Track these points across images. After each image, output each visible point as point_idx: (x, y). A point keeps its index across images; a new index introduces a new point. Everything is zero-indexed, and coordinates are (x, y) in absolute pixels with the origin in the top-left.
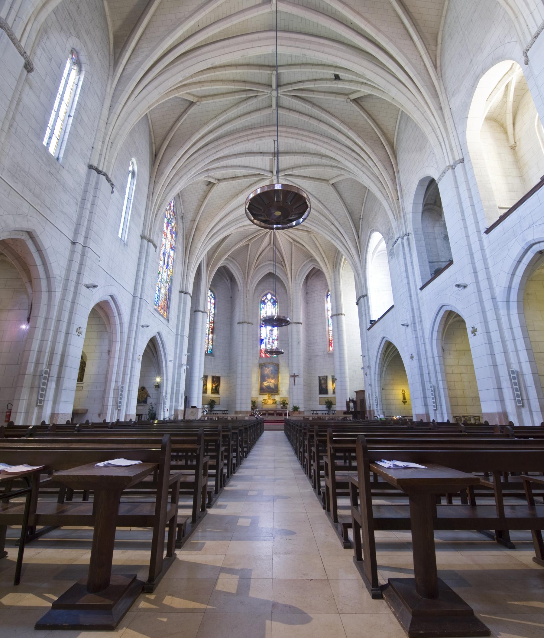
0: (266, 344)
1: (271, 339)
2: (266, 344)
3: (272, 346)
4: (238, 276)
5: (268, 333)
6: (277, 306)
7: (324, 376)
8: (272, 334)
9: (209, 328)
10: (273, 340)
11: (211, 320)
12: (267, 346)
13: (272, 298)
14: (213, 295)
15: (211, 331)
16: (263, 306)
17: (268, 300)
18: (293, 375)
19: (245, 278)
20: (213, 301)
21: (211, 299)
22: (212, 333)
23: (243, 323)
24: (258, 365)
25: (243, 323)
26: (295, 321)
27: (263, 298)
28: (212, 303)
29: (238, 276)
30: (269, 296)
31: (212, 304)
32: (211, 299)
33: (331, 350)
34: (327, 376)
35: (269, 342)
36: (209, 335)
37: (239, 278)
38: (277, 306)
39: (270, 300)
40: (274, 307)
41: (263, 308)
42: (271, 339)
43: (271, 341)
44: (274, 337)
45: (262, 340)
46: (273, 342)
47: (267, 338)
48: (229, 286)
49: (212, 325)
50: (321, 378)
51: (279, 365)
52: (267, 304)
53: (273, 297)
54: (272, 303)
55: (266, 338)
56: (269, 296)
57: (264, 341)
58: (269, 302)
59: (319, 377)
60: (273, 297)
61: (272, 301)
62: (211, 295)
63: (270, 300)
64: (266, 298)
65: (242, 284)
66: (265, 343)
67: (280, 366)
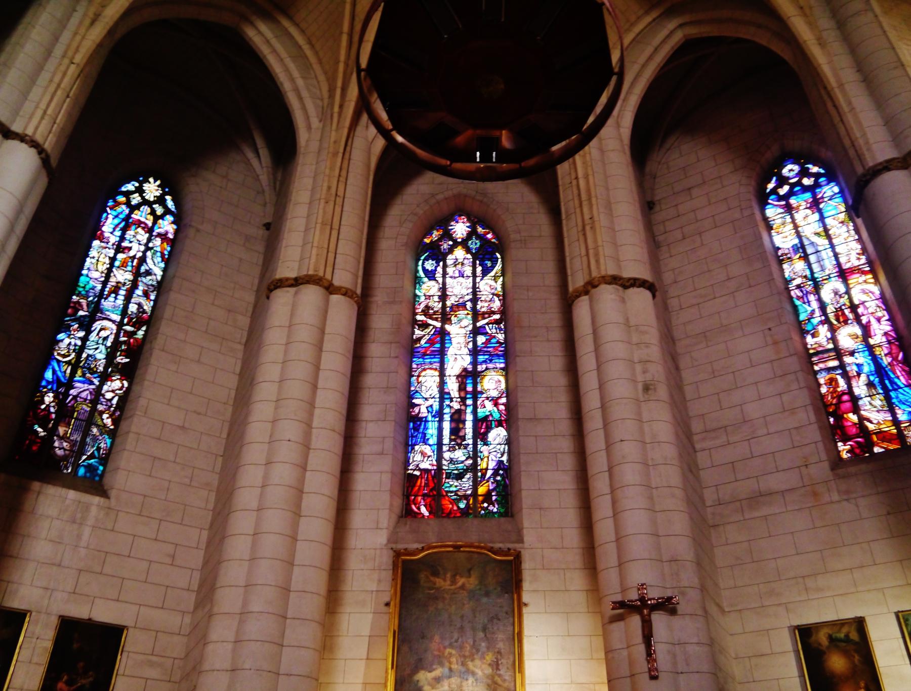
0: (440, 444)
1: (469, 417)
2: (440, 444)
3: (475, 455)
4: (300, 82)
5: (452, 386)
6: (498, 267)
7: (840, 624)
8: (475, 394)
9: (116, 343)
10: (483, 427)
11: (133, 308)
12: (447, 455)
13: (472, 234)
14: (170, 204)
15: (121, 359)
16: (430, 265)
17: (456, 244)
18: (633, 595)
19: (332, 96)
20: (167, 226)
21: (157, 218)
22: (128, 372)
23: (297, 282)
24: (386, 558)
25: (297, 282)
26: (611, 270)
27: (429, 233)
28: (163, 237)
29: (300, 82)
30: (460, 229)
31: (158, 242)
32: (157, 218)
33: (845, 455)
34: (860, 623)
35: (456, 432)
36: (105, 377)
37: (305, 94)
38: (498, 267)
39: (464, 243)
40: (486, 272)
41: (431, 275)
42: (469, 417)
43: (469, 429)
44: (487, 409)
45: (418, 421)
46: (481, 435)
47: (447, 410)
48: (264, 178)
49: (140, 334)
50: (822, 638)
51: (518, 557)
52: (450, 260)
53: (480, 230)
54: (475, 257)
55: (440, 415)
56: (460, 229)
57: (432, 430)
58: (459, 253)
59: (805, 633)
60: (480, 230)
61: (474, 244)
62: (161, 200)
63: (464, 243)
64: (448, 235)
65: (315, 122)
66: (433, 440)
67: (527, 565)
